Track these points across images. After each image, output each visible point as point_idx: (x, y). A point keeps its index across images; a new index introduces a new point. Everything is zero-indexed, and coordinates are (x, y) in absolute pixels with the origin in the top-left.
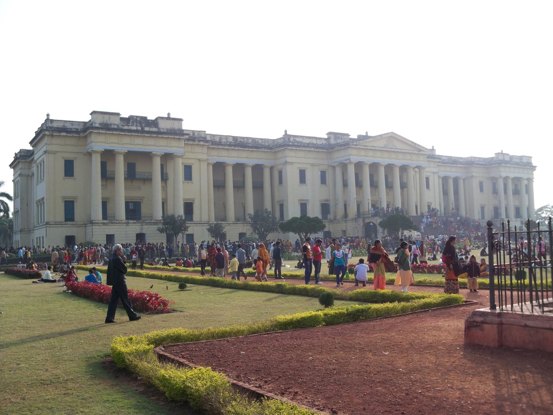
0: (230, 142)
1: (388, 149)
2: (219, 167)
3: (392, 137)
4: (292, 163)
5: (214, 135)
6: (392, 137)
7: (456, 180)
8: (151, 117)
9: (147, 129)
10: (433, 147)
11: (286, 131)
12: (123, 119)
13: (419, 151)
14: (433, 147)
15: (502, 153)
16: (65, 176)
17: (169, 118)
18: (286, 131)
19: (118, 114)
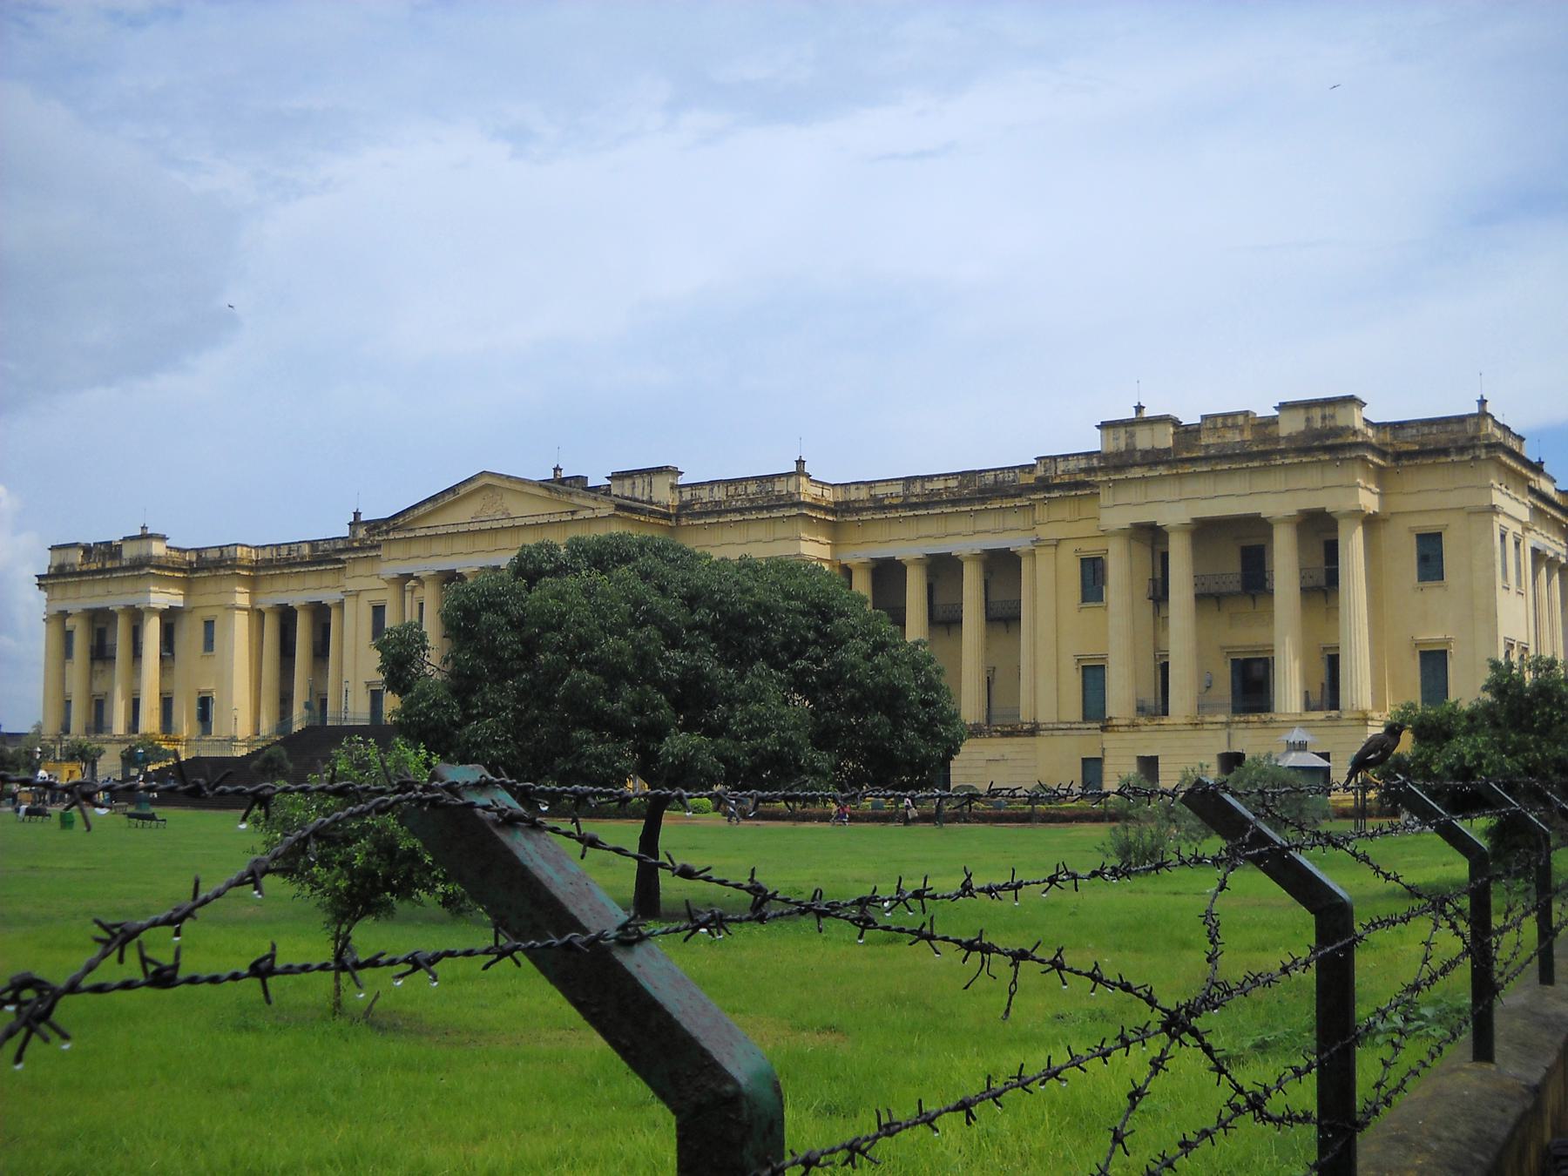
0: (303, 557)
1: (472, 527)
2: (286, 616)
3: (487, 487)
4: (357, 594)
5: (278, 546)
6: (484, 485)
7: (1002, 566)
8: (115, 537)
9: (108, 565)
10: (800, 462)
11: (357, 514)
12: (87, 550)
13: (573, 513)
14: (800, 462)
15: (1141, 421)
16: (1084, 600)
17: (145, 537)
18: (357, 514)
19: (75, 545)
